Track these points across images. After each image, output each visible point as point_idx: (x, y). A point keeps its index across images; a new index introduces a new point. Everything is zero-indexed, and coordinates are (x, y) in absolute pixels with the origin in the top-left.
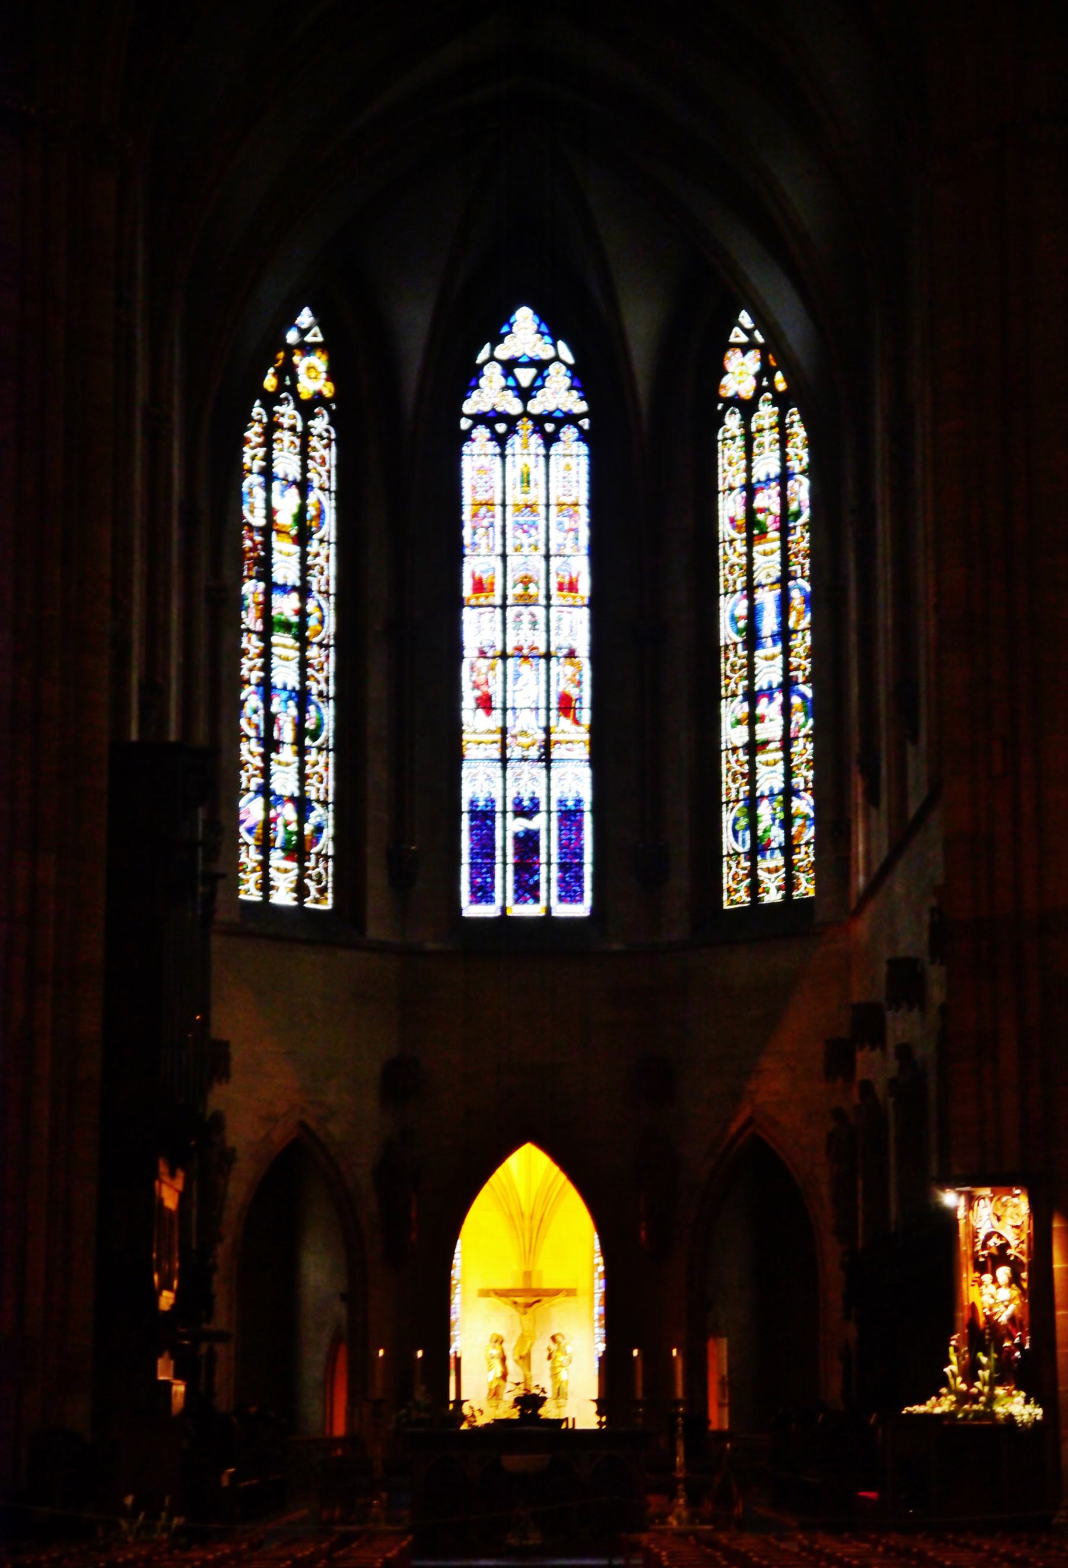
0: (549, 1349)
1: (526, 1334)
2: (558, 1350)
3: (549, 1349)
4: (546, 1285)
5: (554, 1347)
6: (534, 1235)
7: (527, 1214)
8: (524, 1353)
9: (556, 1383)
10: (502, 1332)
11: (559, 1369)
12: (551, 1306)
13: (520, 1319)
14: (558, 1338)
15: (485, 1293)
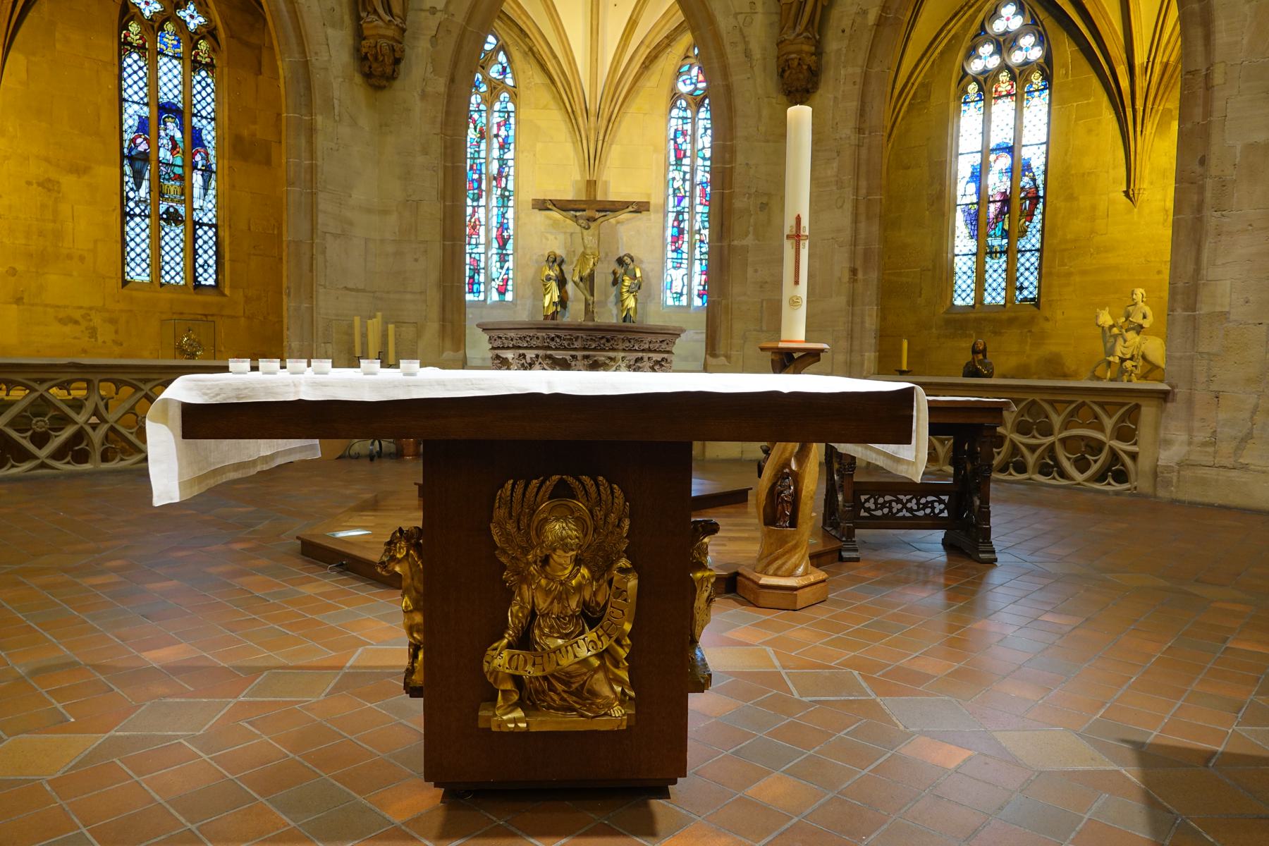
0: (614, 273)
1: (588, 251)
2: (625, 273)
3: (614, 273)
4: (612, 198)
5: (620, 271)
6: (601, 138)
7: (592, 110)
8: (586, 272)
9: (622, 311)
10: (560, 252)
11: (626, 295)
12: (618, 222)
13: (582, 233)
14: (628, 260)
15: (542, 205)
